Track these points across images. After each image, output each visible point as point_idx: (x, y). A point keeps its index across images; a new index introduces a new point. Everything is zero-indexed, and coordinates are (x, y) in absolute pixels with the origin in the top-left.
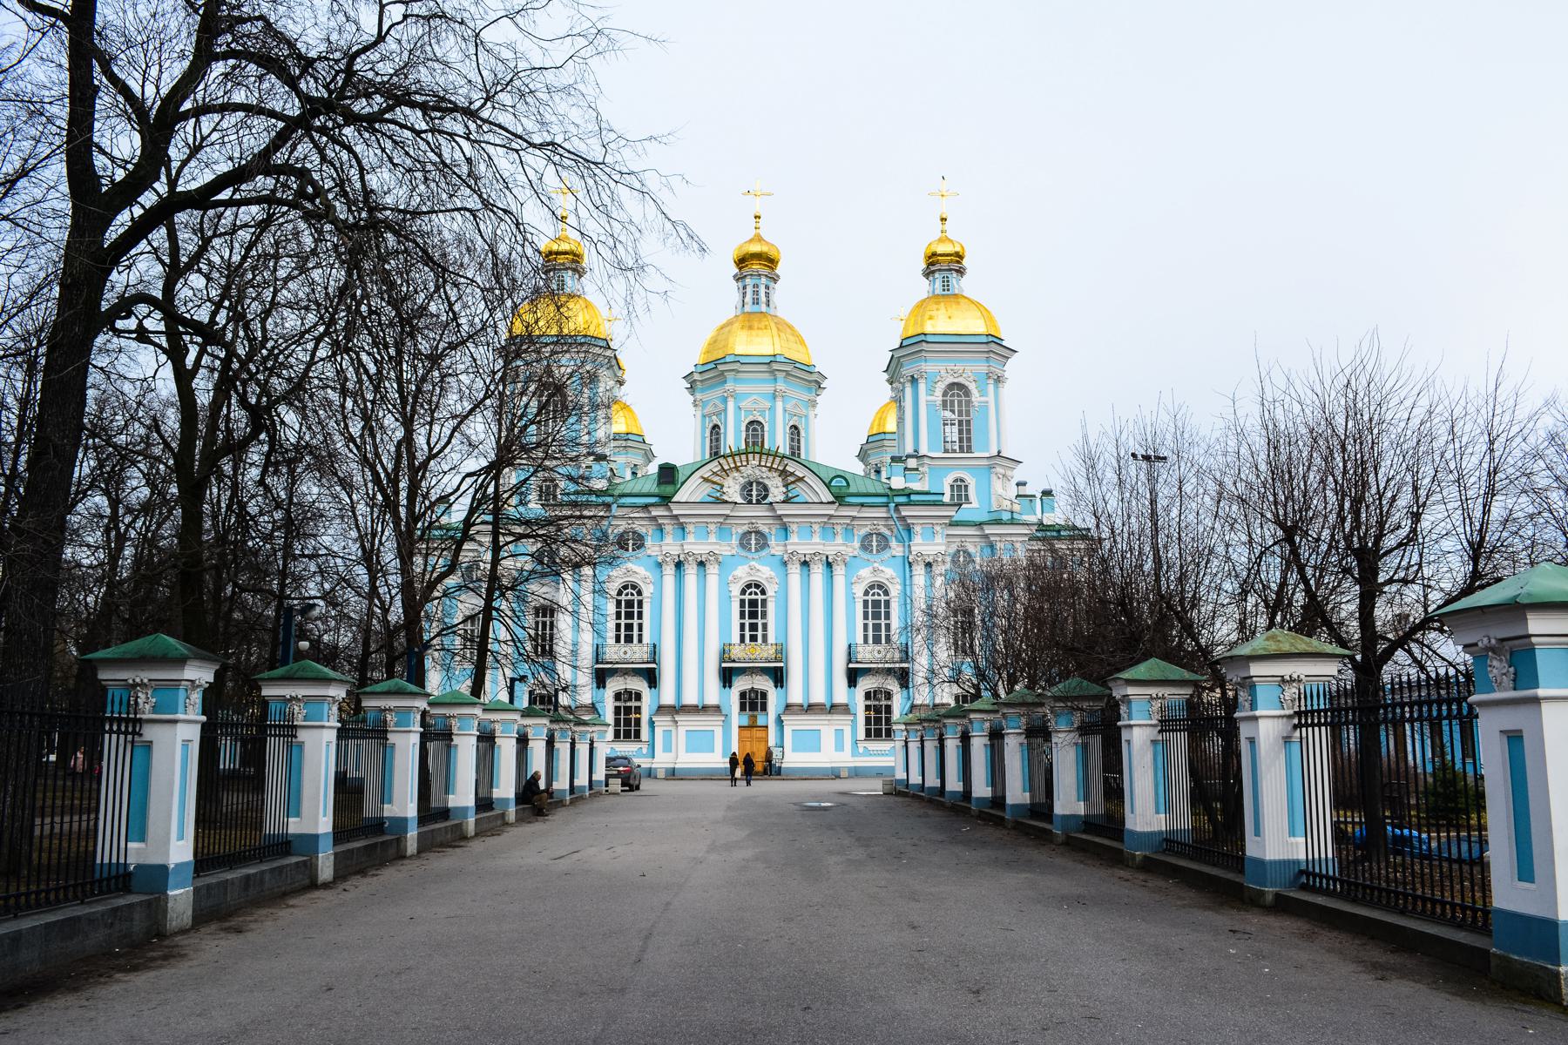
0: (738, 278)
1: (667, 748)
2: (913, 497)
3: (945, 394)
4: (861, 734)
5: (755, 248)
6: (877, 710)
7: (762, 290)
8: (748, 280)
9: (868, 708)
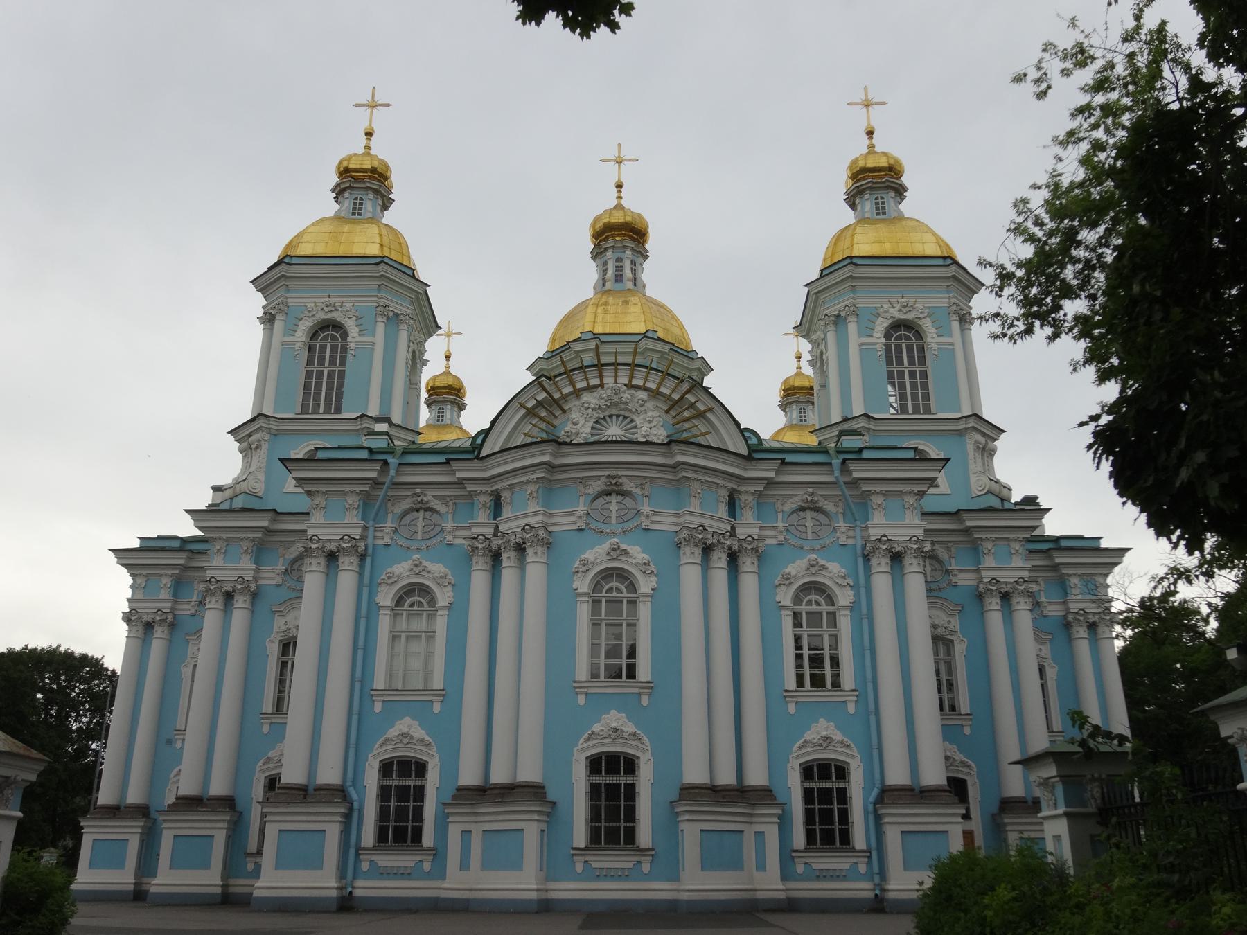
0: (597, 254)
1: (464, 865)
2: (866, 454)
3: (888, 336)
4: (799, 839)
5: (618, 218)
6: (825, 794)
7: (627, 266)
8: (609, 253)
9: (808, 795)
